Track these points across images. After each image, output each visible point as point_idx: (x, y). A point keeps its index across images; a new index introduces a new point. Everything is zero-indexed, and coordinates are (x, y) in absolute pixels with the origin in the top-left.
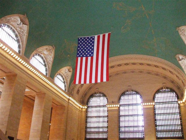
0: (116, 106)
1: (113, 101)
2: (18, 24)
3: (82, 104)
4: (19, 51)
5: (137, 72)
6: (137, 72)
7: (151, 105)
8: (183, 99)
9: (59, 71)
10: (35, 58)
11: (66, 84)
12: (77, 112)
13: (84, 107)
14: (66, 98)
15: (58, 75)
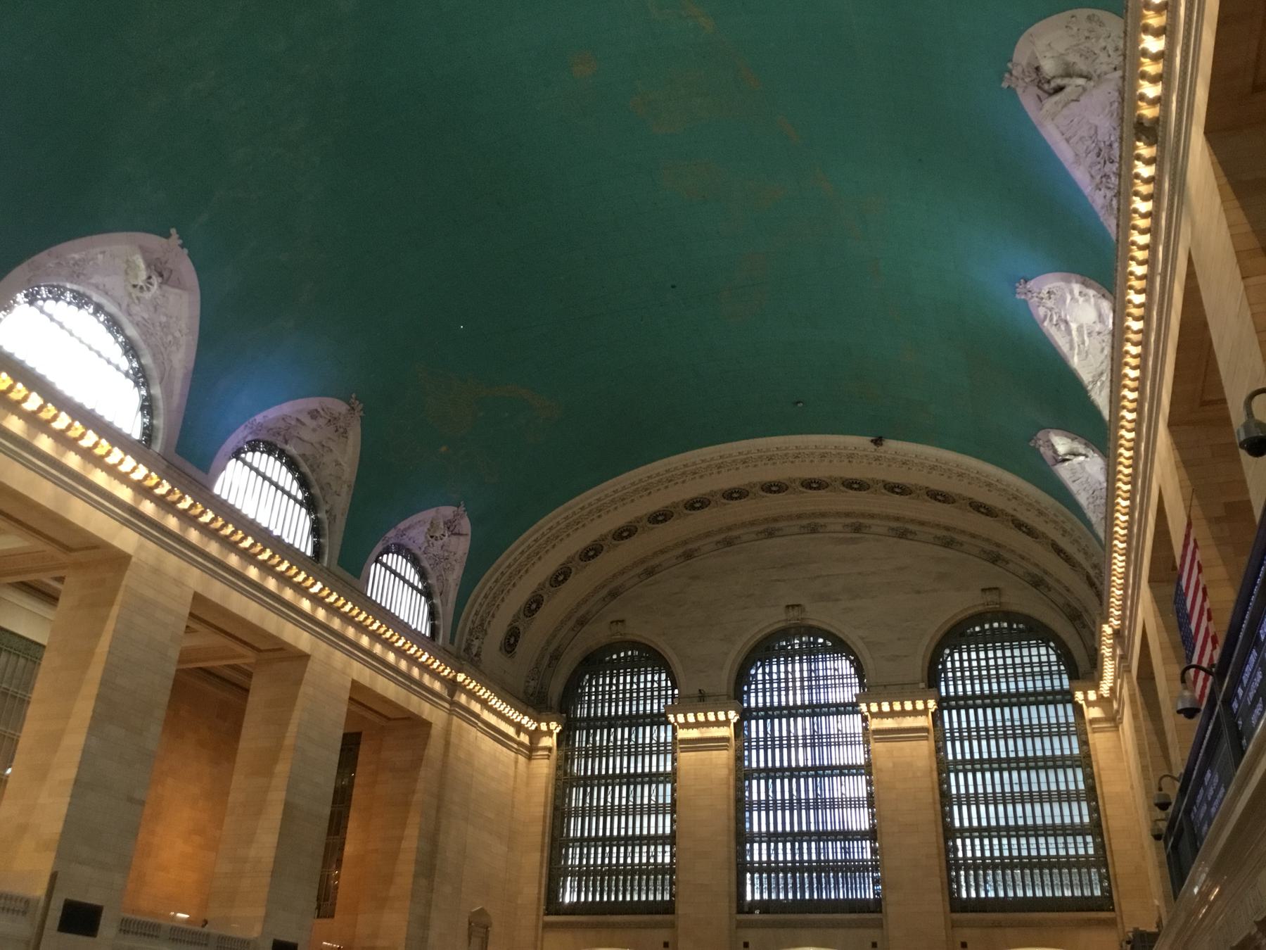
0: (721, 716)
1: (706, 690)
2: (135, 286)
3: (530, 710)
4: (149, 432)
5: (839, 528)
6: (839, 528)
7: (915, 713)
8: (1101, 678)
9: (391, 534)
10: (245, 463)
11: (437, 601)
12: (506, 755)
13: (543, 727)
14: (435, 675)
15: (387, 551)
